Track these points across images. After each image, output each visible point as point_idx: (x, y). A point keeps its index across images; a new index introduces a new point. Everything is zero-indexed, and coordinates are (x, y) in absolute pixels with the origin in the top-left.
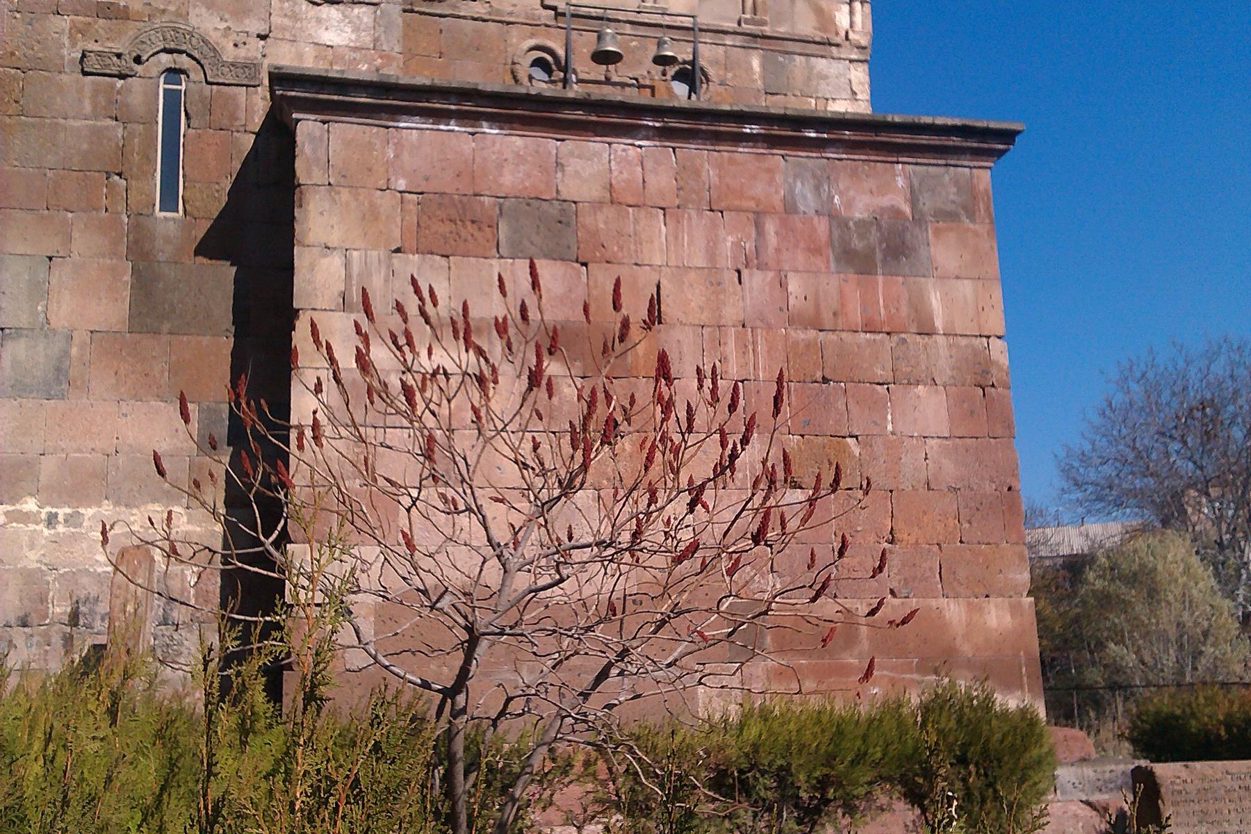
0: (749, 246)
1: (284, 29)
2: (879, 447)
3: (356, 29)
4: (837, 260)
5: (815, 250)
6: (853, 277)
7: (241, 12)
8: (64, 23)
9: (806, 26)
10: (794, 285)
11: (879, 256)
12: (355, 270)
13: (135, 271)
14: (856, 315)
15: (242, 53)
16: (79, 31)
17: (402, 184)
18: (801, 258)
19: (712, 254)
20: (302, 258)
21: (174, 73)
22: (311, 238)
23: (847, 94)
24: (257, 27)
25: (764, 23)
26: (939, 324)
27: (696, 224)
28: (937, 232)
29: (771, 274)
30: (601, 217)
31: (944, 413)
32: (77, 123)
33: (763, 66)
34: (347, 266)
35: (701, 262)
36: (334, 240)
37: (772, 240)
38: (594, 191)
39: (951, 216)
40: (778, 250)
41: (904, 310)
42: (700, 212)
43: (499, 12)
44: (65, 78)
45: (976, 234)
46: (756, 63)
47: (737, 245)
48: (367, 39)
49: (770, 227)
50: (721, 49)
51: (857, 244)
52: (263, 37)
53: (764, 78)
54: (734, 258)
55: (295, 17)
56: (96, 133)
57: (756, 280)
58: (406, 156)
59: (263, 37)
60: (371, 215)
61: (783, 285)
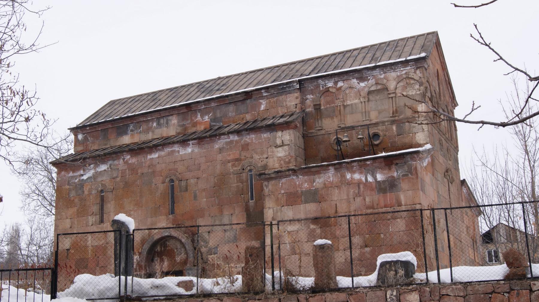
0: (357, 191)
1: (271, 155)
2: (388, 235)
3: (285, 152)
4: (378, 191)
5: (372, 190)
6: (382, 194)
7: (262, 154)
8: (230, 164)
9: (409, 113)
10: (367, 199)
11: (388, 188)
12: (275, 211)
13: (247, 214)
14: (382, 203)
15: (263, 163)
16: (233, 165)
17: (283, 192)
18: (369, 192)
19: (348, 195)
20: (265, 211)
21: (250, 170)
22: (267, 206)
23: (421, 130)
24: (265, 156)
25: (396, 116)
26: (403, 203)
27: (344, 188)
28: (403, 180)
29: (362, 198)
30: (323, 191)
31: (404, 226)
32: (234, 185)
33: (396, 128)
34: (273, 211)
35: (345, 197)
36: (271, 206)
37: (362, 189)
38: (322, 186)
39: (407, 175)
40: (363, 192)
41: (394, 201)
42: (345, 186)
43: (327, 131)
44: (231, 176)
45: (413, 179)
46: (394, 128)
47: (354, 192)
48: (287, 153)
49: (361, 186)
50: (384, 127)
51: (383, 186)
52: (267, 158)
53: (397, 131)
54: (353, 195)
55: (273, 152)
56: (237, 186)
57: (359, 200)
58: (284, 185)
59: (267, 158)
60: (277, 200)
61: (365, 200)
